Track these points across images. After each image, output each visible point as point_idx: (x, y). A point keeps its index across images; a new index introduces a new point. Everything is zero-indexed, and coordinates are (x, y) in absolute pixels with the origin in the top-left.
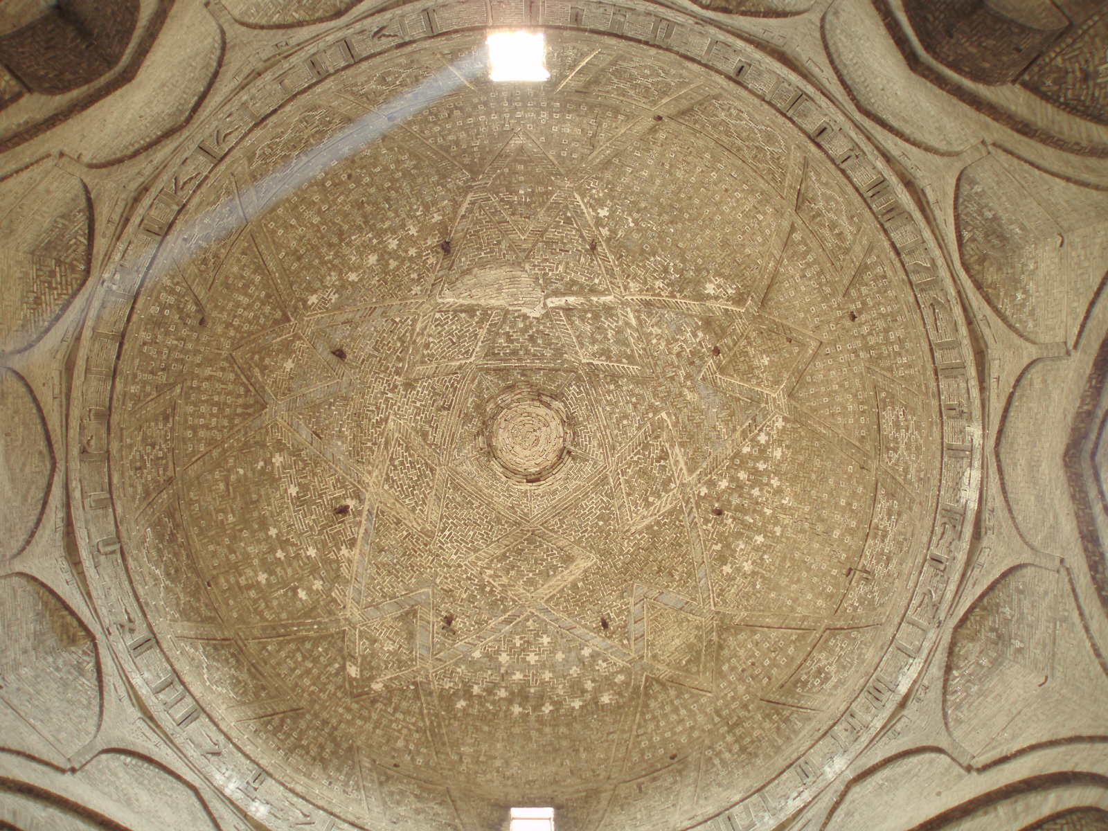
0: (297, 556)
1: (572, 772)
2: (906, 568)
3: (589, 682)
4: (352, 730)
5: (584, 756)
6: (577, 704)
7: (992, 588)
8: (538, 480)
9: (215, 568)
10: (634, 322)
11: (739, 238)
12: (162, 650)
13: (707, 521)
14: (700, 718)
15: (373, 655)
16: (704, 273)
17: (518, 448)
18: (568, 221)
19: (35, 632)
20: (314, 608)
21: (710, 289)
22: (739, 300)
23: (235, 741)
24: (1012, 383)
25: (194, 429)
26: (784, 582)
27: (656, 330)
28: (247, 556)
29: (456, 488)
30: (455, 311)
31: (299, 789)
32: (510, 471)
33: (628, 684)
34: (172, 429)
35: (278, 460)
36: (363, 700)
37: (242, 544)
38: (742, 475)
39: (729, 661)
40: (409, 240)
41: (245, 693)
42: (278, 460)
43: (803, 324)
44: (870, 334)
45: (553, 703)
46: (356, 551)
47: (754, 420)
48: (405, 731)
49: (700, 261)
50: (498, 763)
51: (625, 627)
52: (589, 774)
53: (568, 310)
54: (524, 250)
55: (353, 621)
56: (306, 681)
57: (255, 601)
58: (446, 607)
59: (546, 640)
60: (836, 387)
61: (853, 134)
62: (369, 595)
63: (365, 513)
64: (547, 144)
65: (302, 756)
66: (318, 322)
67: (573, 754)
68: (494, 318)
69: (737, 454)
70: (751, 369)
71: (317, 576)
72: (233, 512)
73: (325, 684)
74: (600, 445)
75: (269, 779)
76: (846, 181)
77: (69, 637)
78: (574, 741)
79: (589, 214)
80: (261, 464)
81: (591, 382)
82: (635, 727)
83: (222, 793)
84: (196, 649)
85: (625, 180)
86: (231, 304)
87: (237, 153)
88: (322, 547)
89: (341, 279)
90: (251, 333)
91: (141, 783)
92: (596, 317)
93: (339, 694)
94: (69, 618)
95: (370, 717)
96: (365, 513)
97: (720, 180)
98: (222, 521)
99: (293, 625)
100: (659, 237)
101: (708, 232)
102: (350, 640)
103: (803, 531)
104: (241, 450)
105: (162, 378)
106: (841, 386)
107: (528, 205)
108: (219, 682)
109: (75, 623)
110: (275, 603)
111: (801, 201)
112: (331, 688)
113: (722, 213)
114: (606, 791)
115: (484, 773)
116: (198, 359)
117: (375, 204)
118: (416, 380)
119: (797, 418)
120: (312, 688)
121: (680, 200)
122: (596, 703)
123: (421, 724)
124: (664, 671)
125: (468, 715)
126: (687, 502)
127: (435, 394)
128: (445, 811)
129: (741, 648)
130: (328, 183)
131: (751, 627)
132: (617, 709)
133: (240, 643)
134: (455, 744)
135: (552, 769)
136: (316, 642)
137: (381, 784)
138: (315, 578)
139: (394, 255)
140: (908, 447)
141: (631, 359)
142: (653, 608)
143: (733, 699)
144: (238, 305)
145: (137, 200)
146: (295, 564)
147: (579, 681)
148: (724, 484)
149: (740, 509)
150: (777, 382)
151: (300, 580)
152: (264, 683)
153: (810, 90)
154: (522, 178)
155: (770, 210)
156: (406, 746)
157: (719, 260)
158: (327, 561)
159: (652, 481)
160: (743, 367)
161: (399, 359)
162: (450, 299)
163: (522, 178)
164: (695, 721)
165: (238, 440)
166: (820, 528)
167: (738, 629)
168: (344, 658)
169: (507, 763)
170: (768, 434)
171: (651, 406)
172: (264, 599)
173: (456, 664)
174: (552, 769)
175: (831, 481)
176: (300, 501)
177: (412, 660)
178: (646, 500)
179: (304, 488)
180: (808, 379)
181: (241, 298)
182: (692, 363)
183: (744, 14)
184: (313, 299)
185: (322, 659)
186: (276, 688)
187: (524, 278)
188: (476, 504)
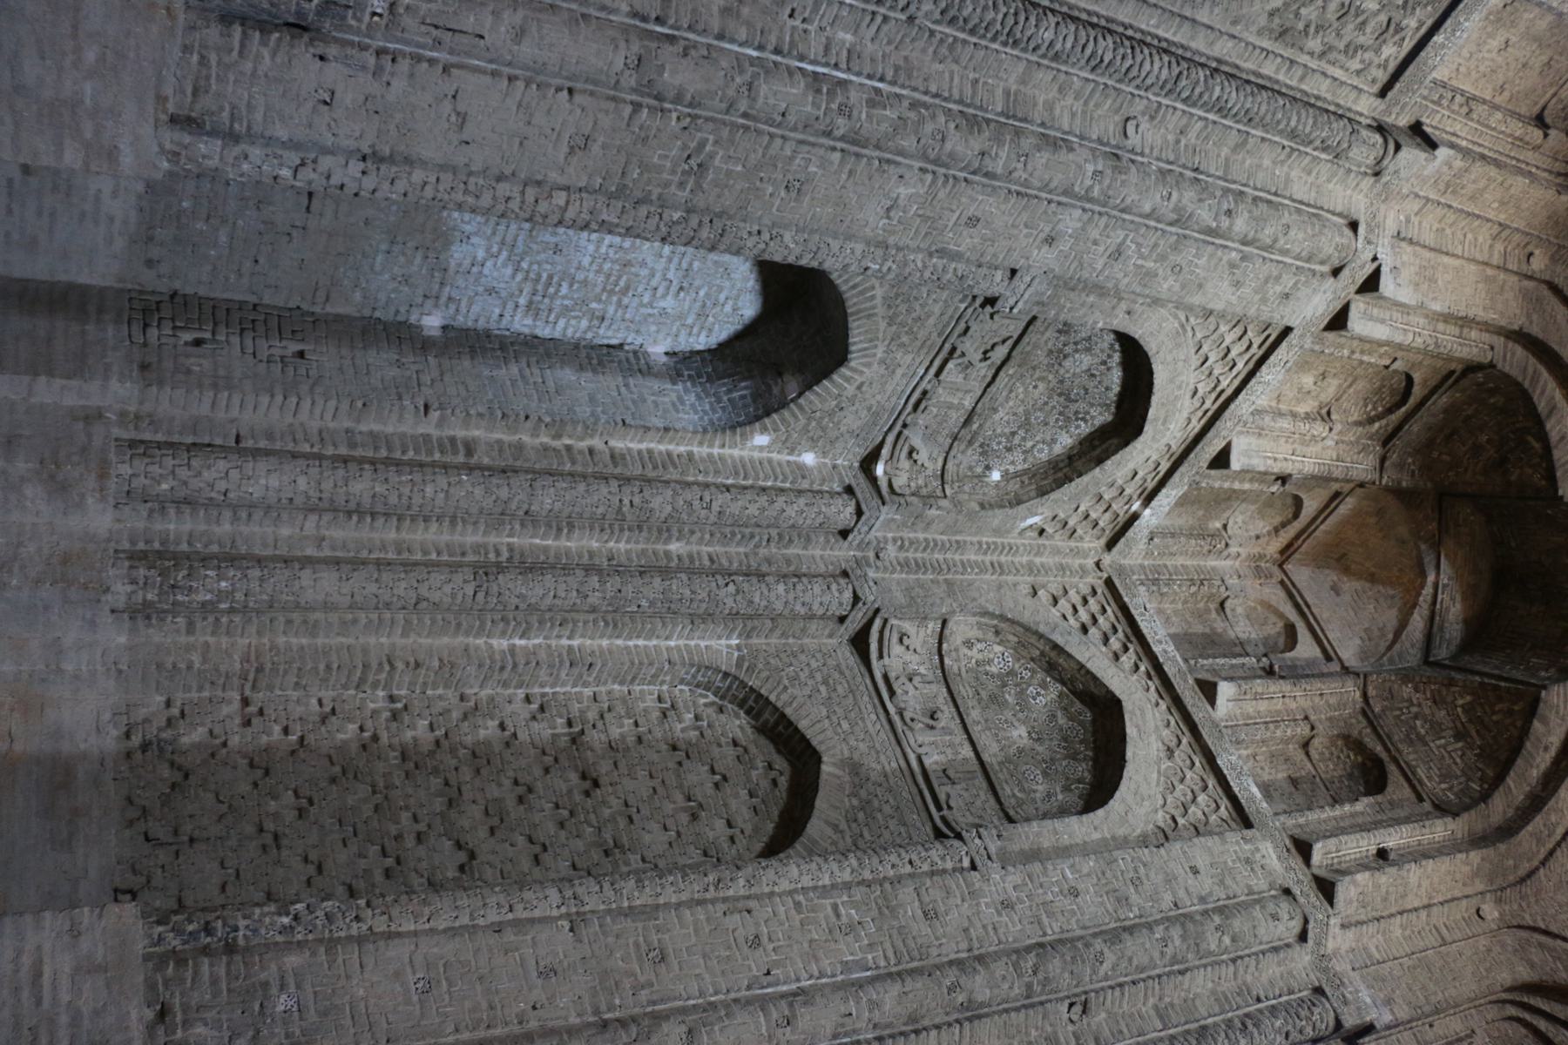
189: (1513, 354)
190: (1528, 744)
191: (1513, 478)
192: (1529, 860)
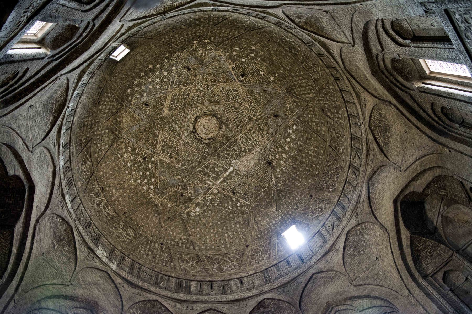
0: (247, 57)
2: (93, 211)
6: (135, 82)
7: (75, 248)
8: (195, 119)
10: (208, 182)
11: (203, 231)
13: (145, 153)
14: (101, 115)
16: (202, 212)
17: (207, 121)
18: (245, 194)
20: (231, 47)
21: (198, 209)
22: (188, 214)
24: (121, 293)
25: (304, 79)
26: (114, 164)
27: (200, 185)
28: (263, 51)
29: (216, 101)
30: (254, 147)
32: (205, 114)
34: (311, 77)
35: (272, 78)
38: (148, 173)
39: (108, 133)
40: (281, 159)
42: (272, 78)
43: (170, 227)
44: (155, 246)
46: (230, 67)
47: (158, 189)
49: (206, 214)
50: (144, 53)
51: (141, 110)
53: (226, 170)
54: (249, 177)
57: (251, 41)
58: (193, 72)
60: (149, 222)
61: (206, 298)
63: (236, 78)
64: (267, 213)
66: (289, 121)
68: (242, 153)
69: (154, 177)
70: (170, 200)
74: (188, 142)
76: (196, 279)
79: (242, 201)
80: (276, 75)
81: (204, 156)
85: (241, 219)
86: (318, 117)
87: (346, 169)
88: (241, 63)
89: (291, 137)
90: (306, 111)
92: (218, 175)
96: (236, 78)
97: (220, 242)
100: (220, 210)
101: (211, 224)
103: (122, 180)
104: (285, 77)
105: (324, 91)
106: (148, 223)
107: (258, 191)
111: (199, 260)
113: (212, 233)
116: (317, 98)
117: (297, 165)
118: (249, 121)
119: (149, 202)
121: (224, 226)
122: (130, 88)
123: (175, 43)
124: (121, 111)
126: (154, 152)
127: (241, 121)
129: (108, 139)
130: (314, 166)
131: (110, 146)
132: (124, 92)
134: (160, 47)
136: (223, 41)
139: (282, 152)
140: (121, 234)
141: (200, 172)
142: (138, 121)
143: (98, 129)
144: (315, 118)
145: (368, 151)
146: (246, 55)
148: (150, 166)
149: (141, 165)
150: (161, 204)
153: (225, 298)
154: (265, 197)
155: (203, 247)
156: (174, 37)
157: (202, 219)
158: (237, 60)
159: (168, 148)
160: (172, 198)
161: (259, 124)
162: (258, 149)
163: (265, 197)
164: (102, 114)
165: (288, 79)
166: (119, 186)
167: (113, 142)
169: (141, 56)
170: (152, 189)
171: (185, 165)
173: (177, 62)
175: (127, 199)
176: (257, 71)
178: (164, 142)
179: (259, 75)
180: (156, 215)
181: (316, 120)
182: (185, 186)
183: (255, 307)
184: (295, 127)
187: (243, 169)
188: (207, 101)
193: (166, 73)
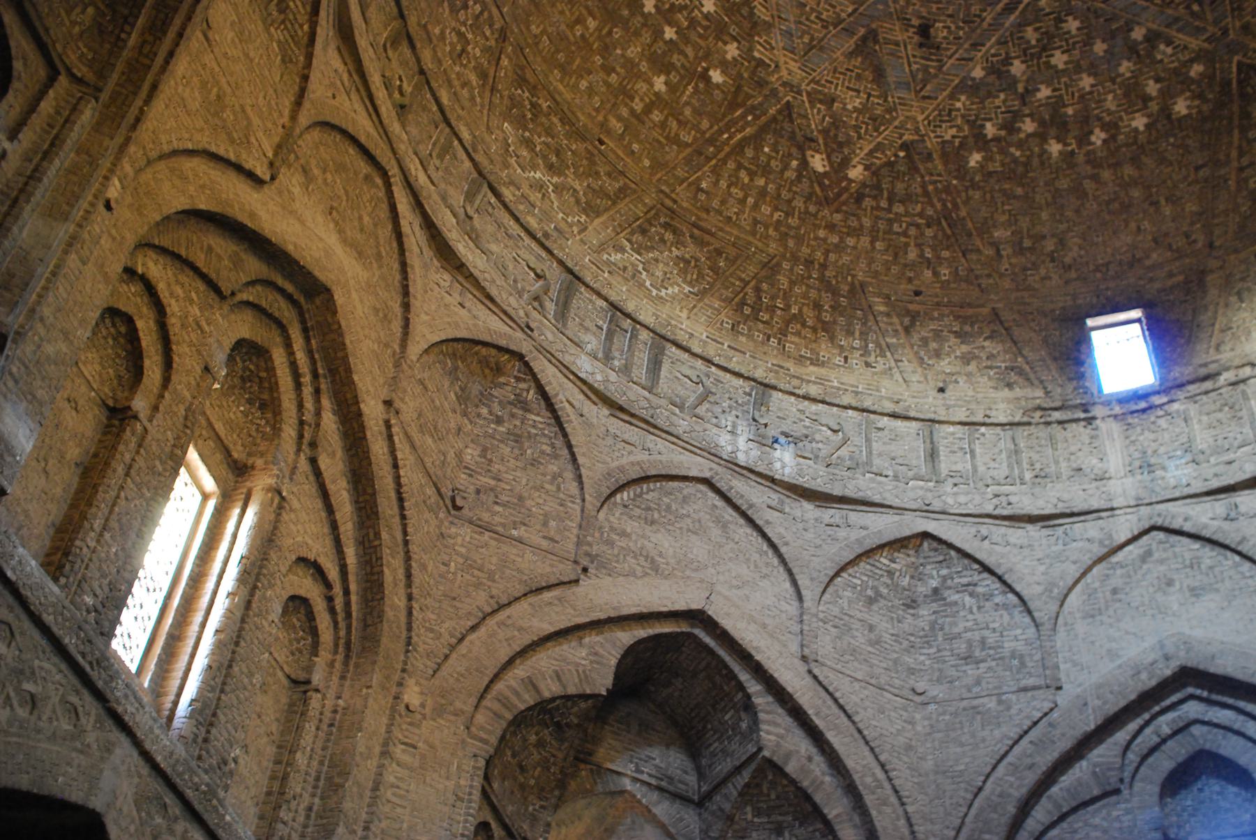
0: (693, 23)
1: (1155, 240)
3: (1151, 82)
4: (846, 259)
5: (1167, 211)
6: (1140, 122)
9: (597, 110)
12: (587, 286)
15: (837, 123)
19: (457, 398)
20: (739, 88)
23: (716, 360)
28: (630, 65)
31: (814, 390)
33: (1211, 77)
36: (844, 203)
37: (619, 51)
41: (701, 276)
45: (1104, 127)
48: (913, 231)
52: (1180, 242)
55: (795, 82)
56: (766, 209)
57: (663, 125)
59: (1073, 25)
62: (804, 32)
65: (798, 334)
67: (1152, 210)
71: (726, 38)
72: (591, 14)
73: (789, 201)
75: (776, 395)
77: (492, 369)
78: (1149, 187)
82: (1234, 154)
83: (737, 465)
84: (622, 250)
91: (653, 522)
93: (812, 209)
94: (484, 351)
95: (862, 226)
98: (582, 36)
99: (721, 132)
102: (800, 115)
108: (664, 283)
109: (493, 352)
110: (688, 112)
112: (799, 203)
114: (1212, 271)
115: (1035, 266)
120: (776, 216)
122: (1169, 117)
123: (930, 212)
125: (990, 174)
128: (1000, 347)
133: (668, 202)
134: (984, 229)
135: (1126, 239)
136: (756, 140)
137: (907, 330)
138: (726, 43)
146: (693, 37)
147: (1137, 84)
151: (706, 57)
152: (717, 245)
156: (922, 256)
168: (801, 149)
169: (1062, 242)
172: (673, 115)
173: (953, 97)
174: (1126, 239)
177: (889, 111)
185: (773, 163)
186: (734, 245)
189: (482, 728)
190: (805, 784)
191: (576, 721)
192: (898, 819)
193: (1017, 68)
